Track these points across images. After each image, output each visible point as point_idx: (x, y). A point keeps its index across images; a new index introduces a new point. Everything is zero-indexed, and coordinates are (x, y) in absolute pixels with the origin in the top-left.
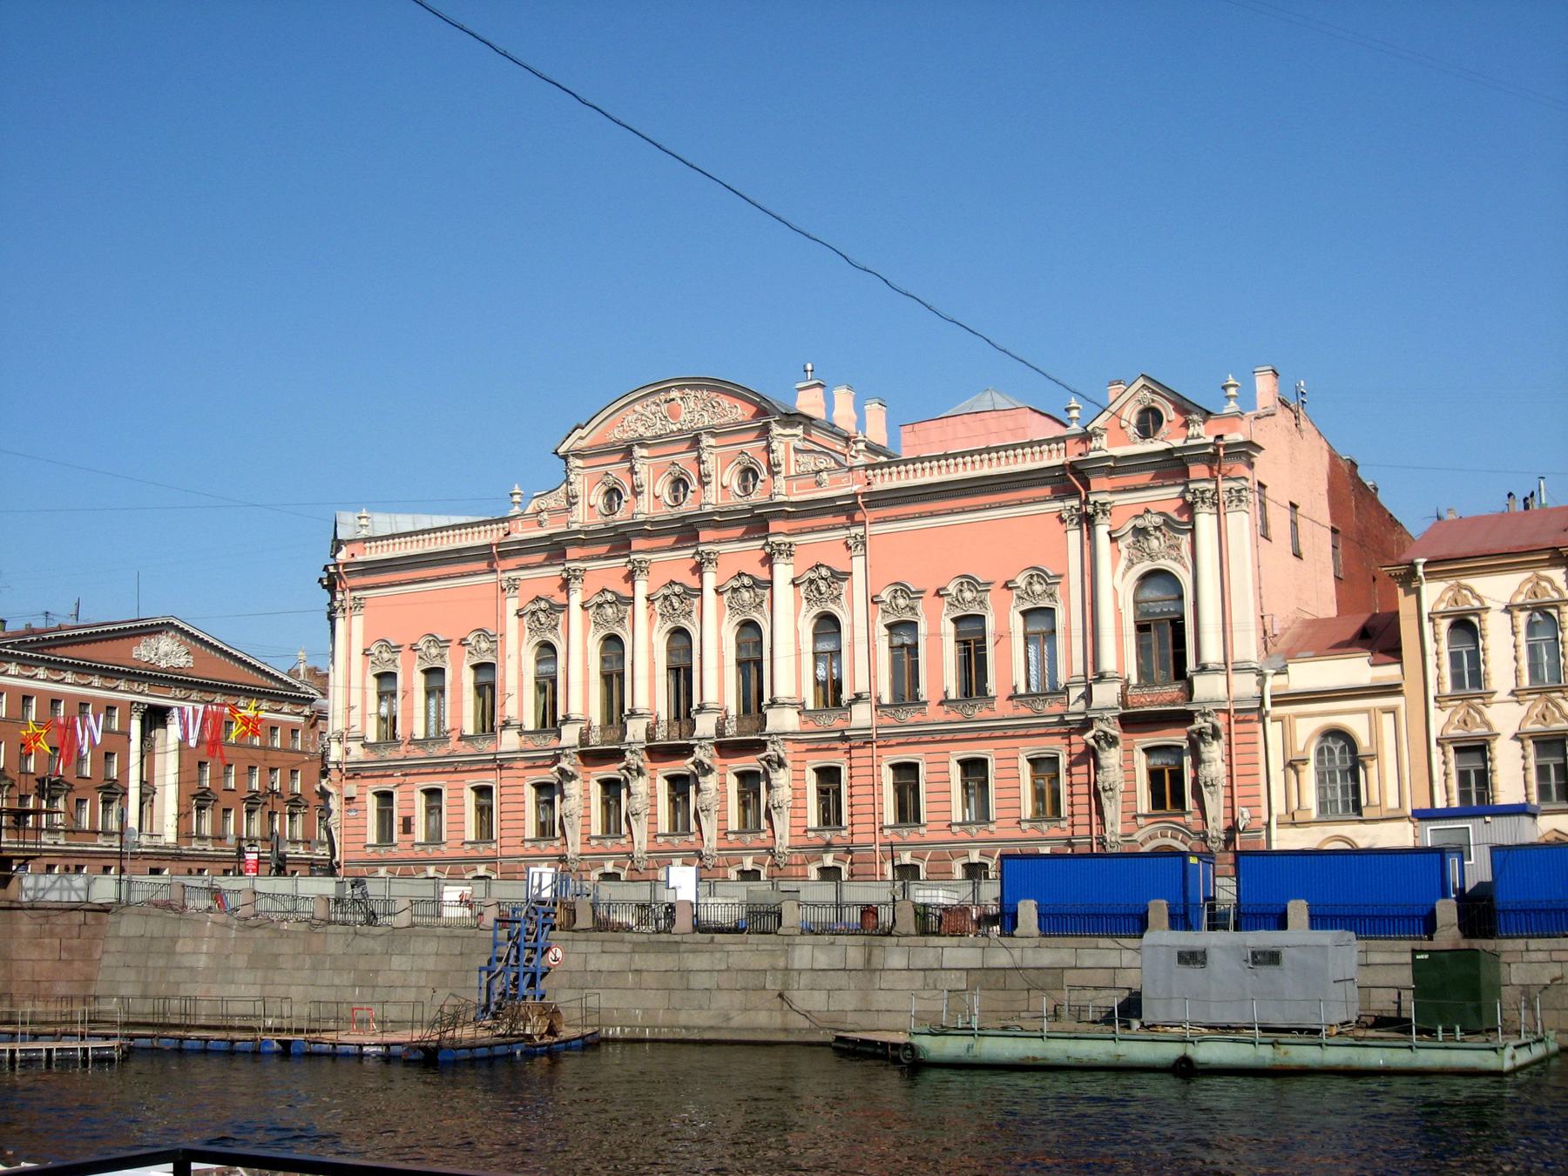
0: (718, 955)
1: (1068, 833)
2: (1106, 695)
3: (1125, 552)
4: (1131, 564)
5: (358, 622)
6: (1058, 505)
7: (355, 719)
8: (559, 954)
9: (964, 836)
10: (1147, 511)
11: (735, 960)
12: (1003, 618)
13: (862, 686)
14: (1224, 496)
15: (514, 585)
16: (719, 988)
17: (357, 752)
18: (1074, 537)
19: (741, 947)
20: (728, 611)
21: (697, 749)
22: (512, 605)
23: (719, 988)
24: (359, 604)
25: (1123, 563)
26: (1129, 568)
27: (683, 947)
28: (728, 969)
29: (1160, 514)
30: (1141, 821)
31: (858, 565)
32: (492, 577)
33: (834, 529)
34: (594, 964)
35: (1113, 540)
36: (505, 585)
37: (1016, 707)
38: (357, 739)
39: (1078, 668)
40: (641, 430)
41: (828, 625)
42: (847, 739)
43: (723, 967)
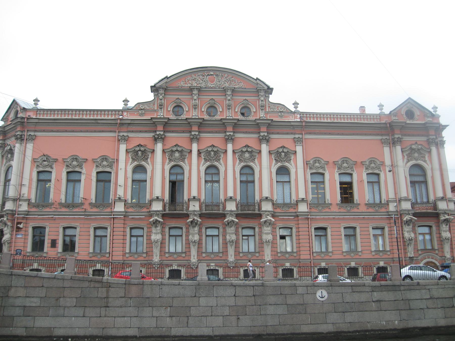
0: (423, 291)
1: (391, 257)
2: (406, 206)
3: (406, 157)
4: (408, 161)
5: (30, 146)
6: (380, 137)
7: (25, 191)
8: (325, 293)
9: (348, 257)
10: (416, 143)
11: (435, 293)
12: (360, 176)
13: (302, 195)
14: (439, 142)
15: (126, 139)
16: (428, 308)
17: (24, 207)
18: (386, 150)
19: (436, 287)
20: (238, 161)
21: (228, 216)
22: (123, 147)
23: (428, 308)
24: (32, 139)
25: (405, 160)
26: (407, 162)
27: (402, 288)
28: (431, 298)
29: (420, 145)
30: (420, 252)
31: (299, 149)
33: (287, 134)
34: (348, 298)
35: (402, 152)
36: (120, 138)
37: (368, 209)
38: (25, 200)
39: (392, 195)
40: (196, 85)
41: (283, 171)
42: (297, 216)
43: (428, 297)
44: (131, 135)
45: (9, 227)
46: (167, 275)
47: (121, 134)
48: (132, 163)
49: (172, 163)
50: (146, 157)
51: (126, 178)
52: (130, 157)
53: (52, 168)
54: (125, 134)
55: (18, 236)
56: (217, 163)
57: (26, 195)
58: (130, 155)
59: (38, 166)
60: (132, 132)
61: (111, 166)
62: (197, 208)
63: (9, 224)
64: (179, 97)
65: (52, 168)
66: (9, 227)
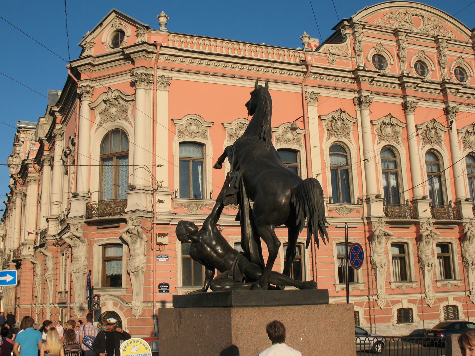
5: (163, 96)
32: (298, 89)
44: (323, 92)
45: (143, 243)
46: (396, 319)
47: (310, 90)
48: (328, 139)
49: (383, 142)
50: (347, 131)
51: (323, 162)
52: (325, 129)
53: (205, 138)
54: (316, 90)
55: (160, 259)
56: (438, 147)
57: (165, 184)
58: (324, 123)
59: (180, 132)
60: (324, 87)
61: (298, 142)
62: (428, 214)
63: (144, 236)
64: (383, 42)
65: (205, 138)
66: (143, 243)
